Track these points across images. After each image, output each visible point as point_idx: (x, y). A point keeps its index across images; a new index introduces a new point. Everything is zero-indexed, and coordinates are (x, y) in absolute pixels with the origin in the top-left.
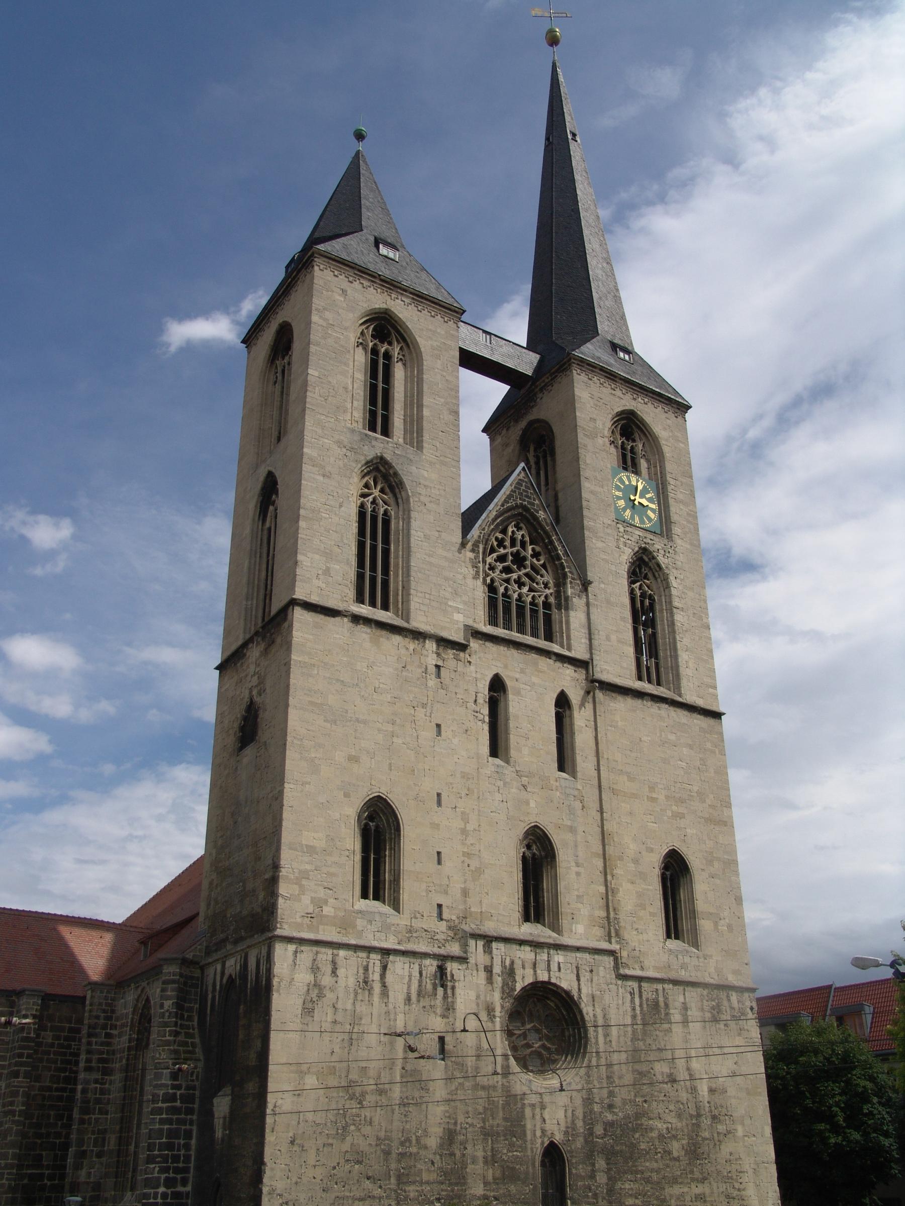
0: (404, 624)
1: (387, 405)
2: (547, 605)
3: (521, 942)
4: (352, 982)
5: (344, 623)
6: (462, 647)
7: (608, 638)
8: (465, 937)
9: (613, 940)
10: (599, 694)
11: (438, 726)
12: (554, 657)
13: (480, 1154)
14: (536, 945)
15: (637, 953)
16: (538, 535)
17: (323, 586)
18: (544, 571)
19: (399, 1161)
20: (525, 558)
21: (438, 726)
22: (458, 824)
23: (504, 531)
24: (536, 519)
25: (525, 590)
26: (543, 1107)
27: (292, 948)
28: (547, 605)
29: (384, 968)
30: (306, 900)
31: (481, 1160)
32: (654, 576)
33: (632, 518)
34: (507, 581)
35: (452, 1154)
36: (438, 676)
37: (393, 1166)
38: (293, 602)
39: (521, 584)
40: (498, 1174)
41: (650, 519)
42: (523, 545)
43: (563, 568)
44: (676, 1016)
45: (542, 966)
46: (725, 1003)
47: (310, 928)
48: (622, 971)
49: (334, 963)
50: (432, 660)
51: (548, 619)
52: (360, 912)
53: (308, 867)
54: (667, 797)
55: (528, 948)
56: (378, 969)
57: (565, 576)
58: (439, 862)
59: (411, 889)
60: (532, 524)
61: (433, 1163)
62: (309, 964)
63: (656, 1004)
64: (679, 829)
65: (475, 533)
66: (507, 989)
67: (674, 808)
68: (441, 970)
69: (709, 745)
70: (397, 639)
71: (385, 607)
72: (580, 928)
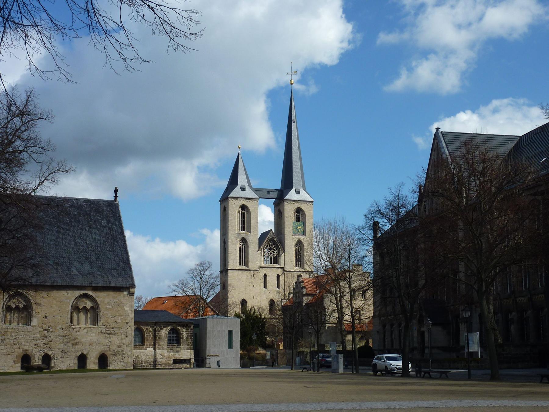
0: (247, 268)
1: (244, 224)
10: (285, 273)
16: (274, 243)
28: (276, 257)
39: (271, 254)
50: (252, 274)
51: (276, 259)
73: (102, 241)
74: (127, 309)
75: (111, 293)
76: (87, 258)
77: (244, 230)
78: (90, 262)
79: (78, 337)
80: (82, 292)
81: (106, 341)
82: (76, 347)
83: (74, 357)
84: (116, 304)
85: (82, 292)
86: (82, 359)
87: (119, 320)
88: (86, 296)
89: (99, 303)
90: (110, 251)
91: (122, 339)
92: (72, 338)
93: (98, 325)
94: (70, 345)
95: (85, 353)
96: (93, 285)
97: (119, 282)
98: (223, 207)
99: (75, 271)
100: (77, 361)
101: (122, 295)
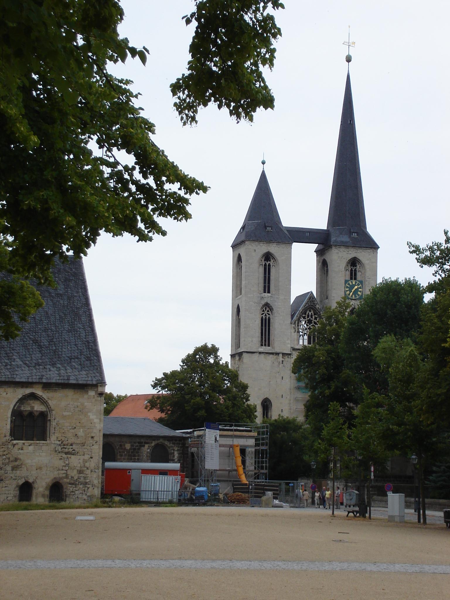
5: (257, 354)
6: (290, 354)
41: (358, 295)
42: (312, 317)
65: (295, 318)
70: (271, 356)
71: (269, 346)
73: (58, 317)
74: (92, 416)
75: (70, 393)
76: (35, 341)
77: (269, 292)
78: (40, 347)
79: (19, 457)
80: (28, 391)
81: (61, 463)
82: (18, 472)
83: (14, 486)
84: (77, 409)
85: (28, 391)
86: (26, 490)
87: (81, 433)
88: (33, 396)
89: (52, 407)
90: (69, 331)
91: (85, 461)
92: (11, 459)
93: (50, 440)
94: (9, 468)
95: (31, 481)
96: (44, 381)
97: (83, 377)
98: (237, 255)
99: (18, 360)
100: (18, 492)
101: (86, 396)
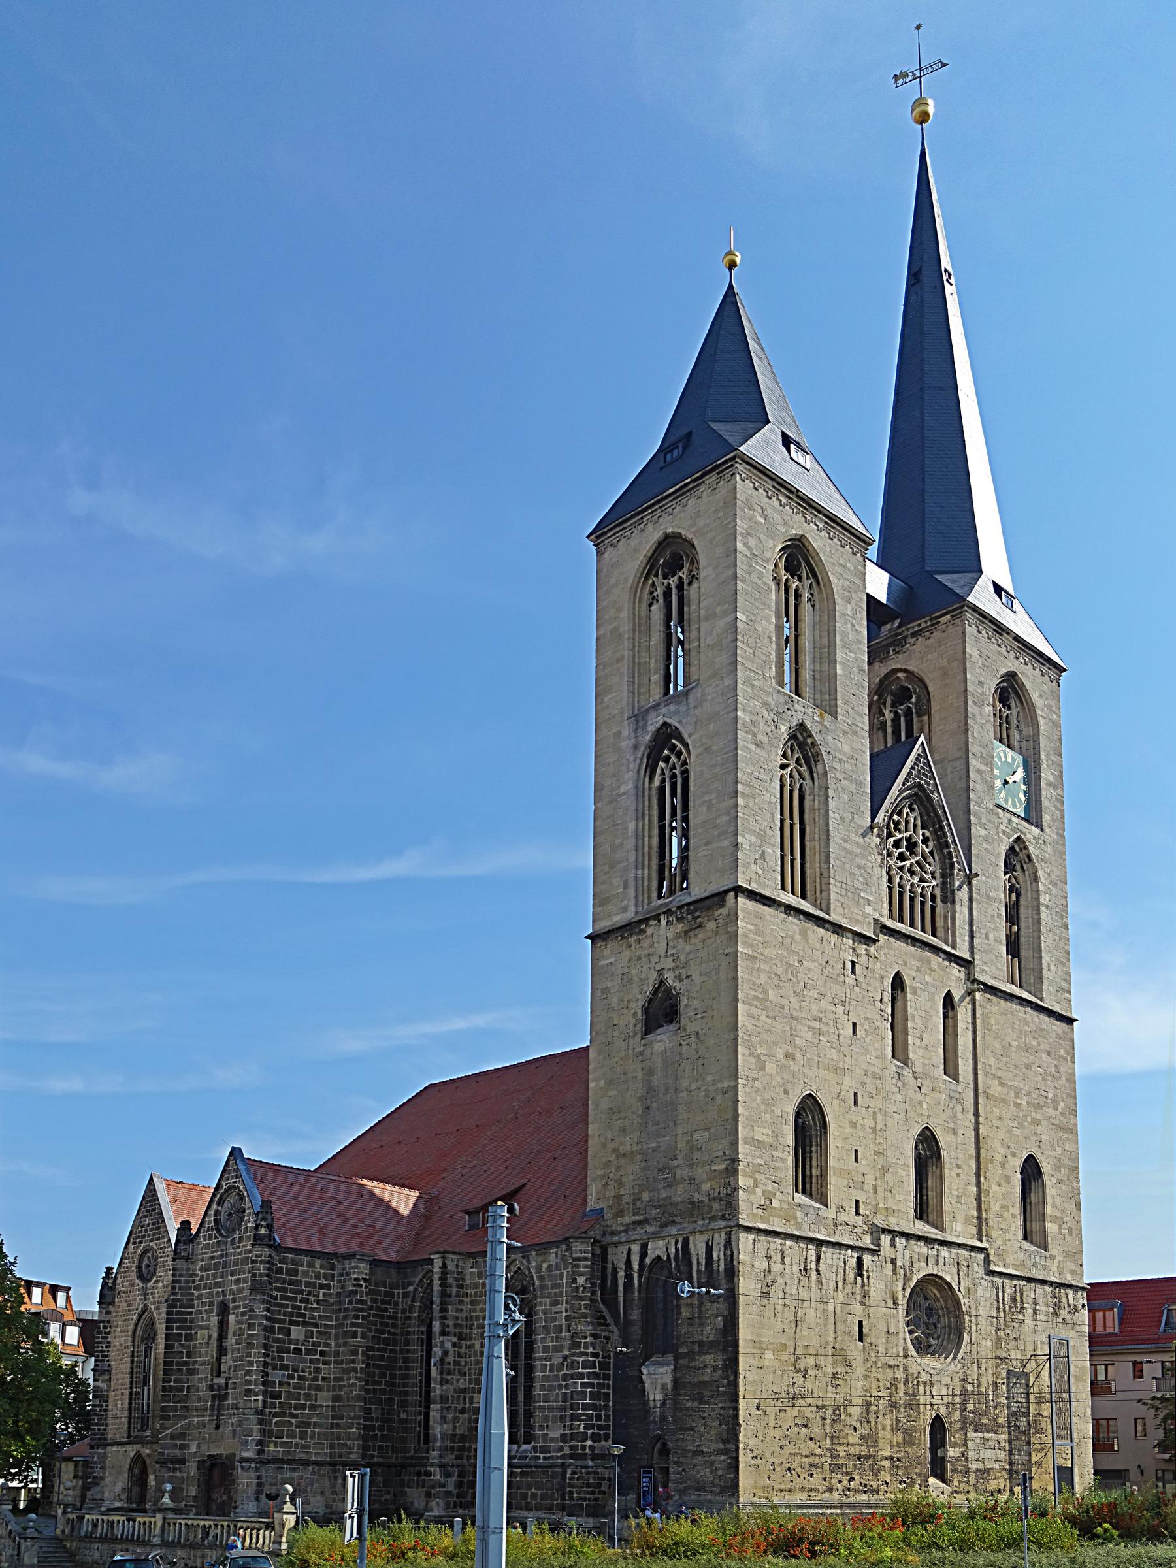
2: (933, 897)
3: (919, 1238)
4: (796, 1268)
7: (987, 937)
8: (877, 1232)
9: (984, 1239)
11: (854, 1025)
12: (942, 955)
13: (888, 1422)
14: (927, 1240)
15: (1000, 1252)
17: (760, 871)
18: (931, 860)
19: (832, 1426)
20: (915, 844)
21: (854, 1025)
22: (869, 1123)
23: (900, 814)
24: (930, 800)
25: (916, 880)
26: (932, 1386)
27: (751, 1237)
29: (818, 1258)
30: (759, 1191)
31: (888, 1428)
32: (1022, 867)
33: (1006, 801)
34: (901, 868)
35: (868, 1422)
36: (853, 972)
37: (829, 1430)
38: (738, 890)
39: (913, 873)
40: (900, 1440)
43: (951, 857)
44: (1029, 1311)
45: (932, 1260)
46: (1064, 1300)
47: (765, 1220)
48: (993, 1268)
49: (782, 1252)
50: (849, 957)
52: (799, 1205)
53: (760, 1162)
54: (1028, 1103)
55: (921, 1243)
56: (814, 1259)
57: (952, 866)
58: (856, 1160)
59: (836, 1186)
60: (925, 807)
61: (855, 1429)
62: (764, 1253)
63: (1014, 1300)
64: (1036, 1134)
66: (906, 1279)
67: (1033, 1114)
68: (860, 1261)
69: (1062, 1052)
72: (959, 1230)
